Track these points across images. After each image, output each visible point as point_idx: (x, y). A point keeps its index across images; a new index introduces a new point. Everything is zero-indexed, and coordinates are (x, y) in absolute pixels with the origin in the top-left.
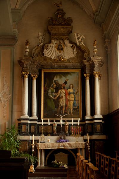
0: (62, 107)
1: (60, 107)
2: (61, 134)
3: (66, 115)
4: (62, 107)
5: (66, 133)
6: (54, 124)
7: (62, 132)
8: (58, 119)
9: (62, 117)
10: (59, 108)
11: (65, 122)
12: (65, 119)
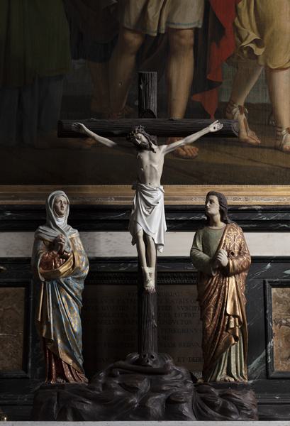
0: (158, 50)
1: (134, 40)
2: (144, 385)
3: (215, 127)
4: (158, 50)
5: (221, 376)
6: (55, 245)
7: (154, 363)
8: (112, 195)
9: (155, 160)
10: (126, 64)
11: (210, 221)
12: (193, 195)
